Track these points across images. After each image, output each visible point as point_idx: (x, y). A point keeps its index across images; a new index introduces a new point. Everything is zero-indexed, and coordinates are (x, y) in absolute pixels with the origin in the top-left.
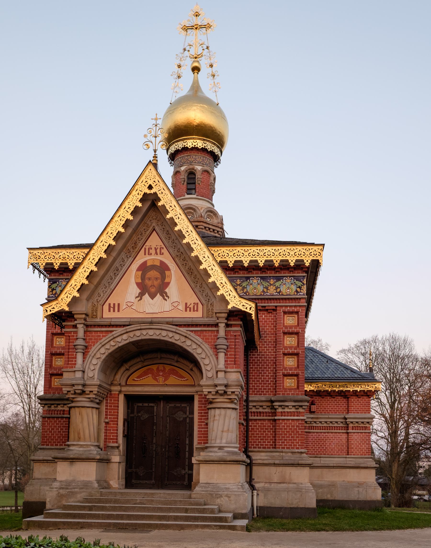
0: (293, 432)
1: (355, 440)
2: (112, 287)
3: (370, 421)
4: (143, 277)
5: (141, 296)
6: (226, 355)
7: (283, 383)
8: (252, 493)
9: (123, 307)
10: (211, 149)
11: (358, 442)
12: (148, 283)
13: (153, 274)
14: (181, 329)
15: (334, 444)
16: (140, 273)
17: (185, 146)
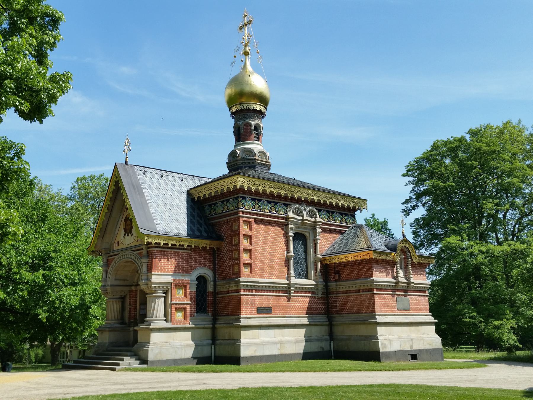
0: (236, 303)
1: (365, 300)
2: (116, 233)
3: (371, 284)
4: (126, 225)
5: (125, 235)
6: (148, 265)
7: (233, 270)
8: (212, 347)
9: (120, 243)
10: (247, 108)
11: (367, 302)
12: (127, 228)
13: (129, 222)
14: (134, 252)
15: (353, 304)
16: (125, 222)
17: (242, 108)
